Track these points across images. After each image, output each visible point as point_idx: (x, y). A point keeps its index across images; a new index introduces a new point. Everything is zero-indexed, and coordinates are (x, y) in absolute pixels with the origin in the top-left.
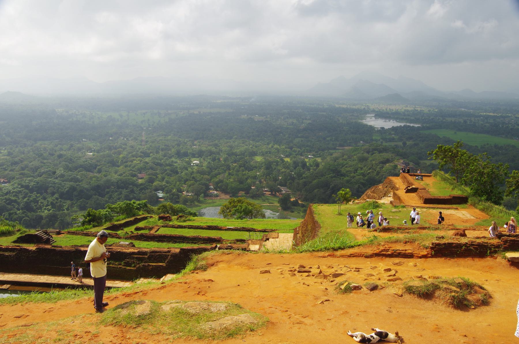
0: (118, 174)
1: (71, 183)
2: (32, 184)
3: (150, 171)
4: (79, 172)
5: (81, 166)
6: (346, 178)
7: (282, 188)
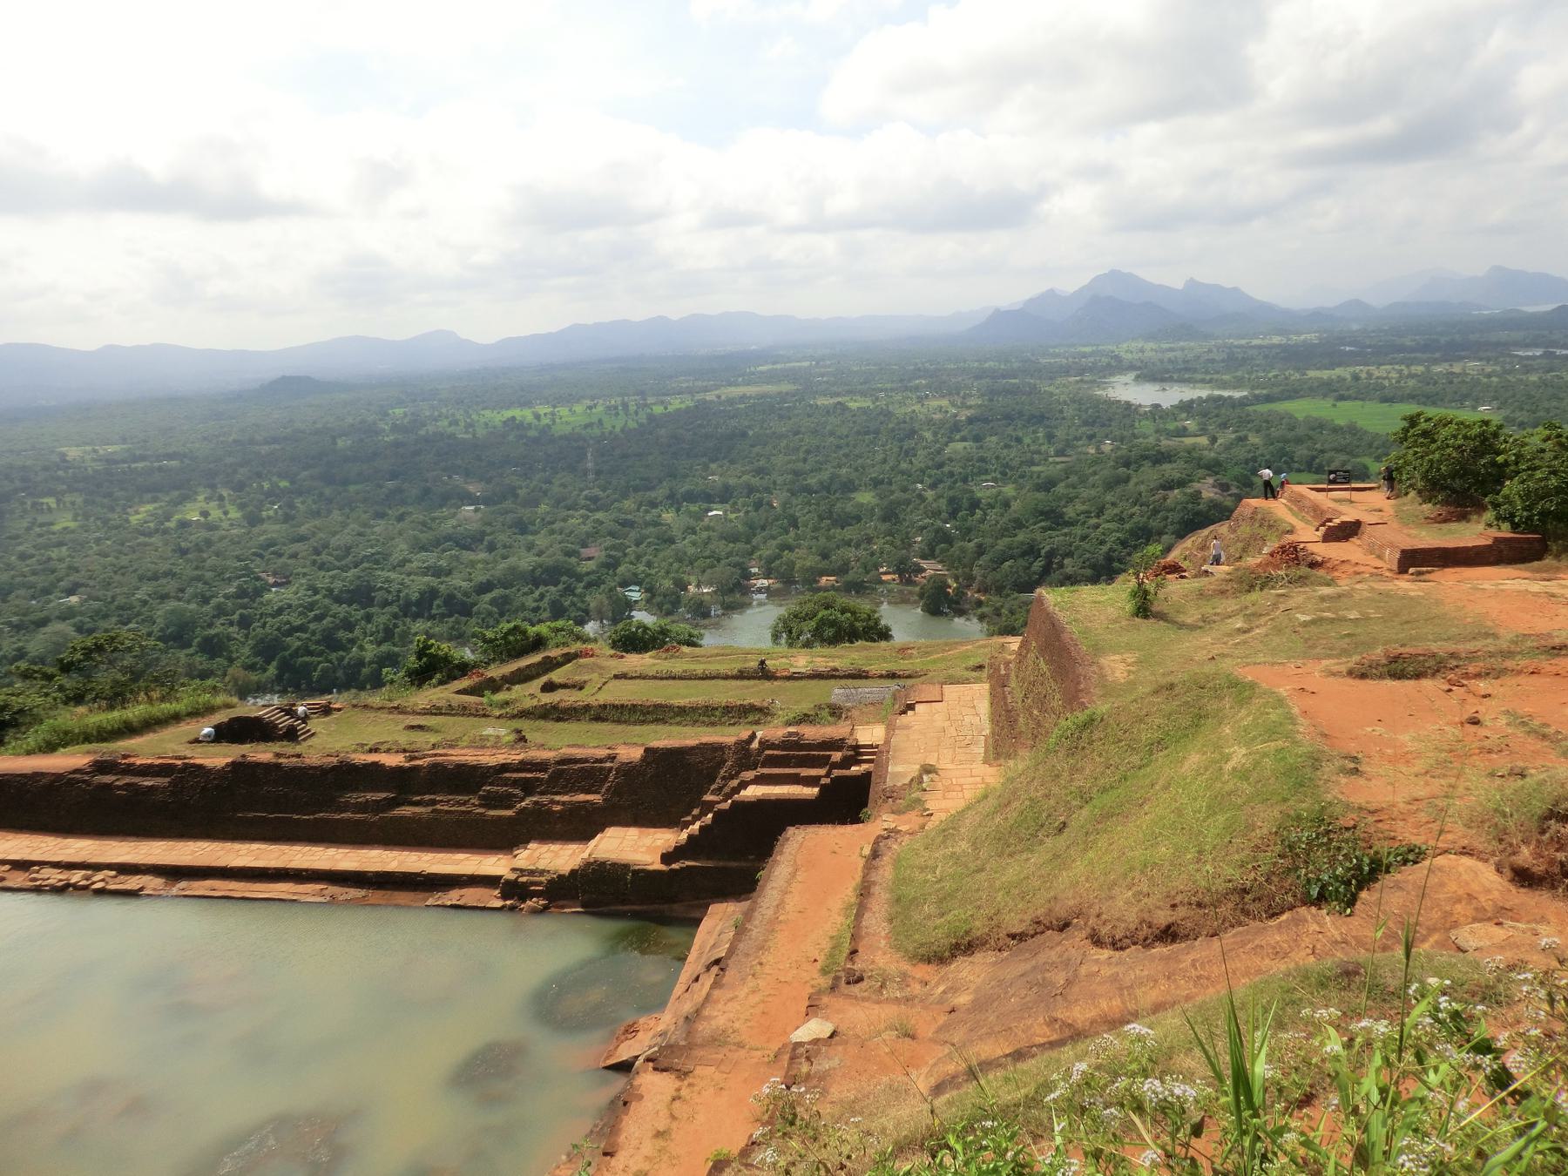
0: (534, 551)
1: (427, 579)
2: (338, 585)
3: (609, 541)
4: (444, 551)
5: (448, 538)
6: (1078, 531)
7: (924, 564)
